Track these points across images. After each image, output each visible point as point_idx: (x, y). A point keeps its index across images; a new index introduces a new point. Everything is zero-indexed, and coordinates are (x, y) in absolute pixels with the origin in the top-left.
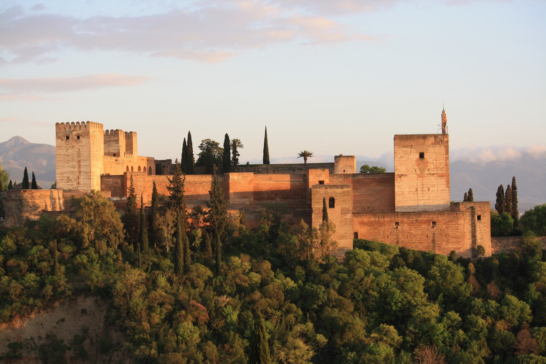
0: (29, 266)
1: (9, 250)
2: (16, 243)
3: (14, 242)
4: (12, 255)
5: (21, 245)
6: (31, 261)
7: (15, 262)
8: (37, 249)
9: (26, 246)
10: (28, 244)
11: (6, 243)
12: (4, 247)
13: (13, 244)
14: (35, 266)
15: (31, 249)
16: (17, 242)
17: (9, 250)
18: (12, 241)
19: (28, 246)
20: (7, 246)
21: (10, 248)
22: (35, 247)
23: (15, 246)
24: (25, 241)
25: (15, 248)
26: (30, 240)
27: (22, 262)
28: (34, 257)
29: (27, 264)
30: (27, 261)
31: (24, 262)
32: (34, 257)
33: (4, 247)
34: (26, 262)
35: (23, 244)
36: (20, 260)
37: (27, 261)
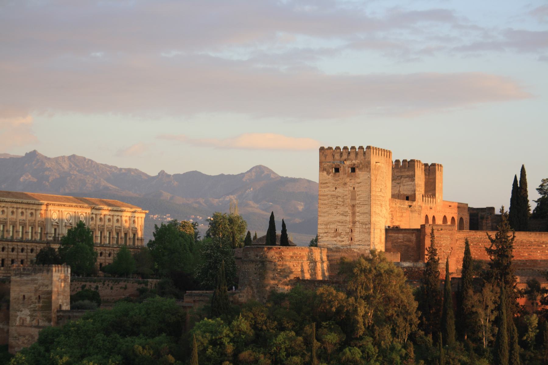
0: (272, 361)
1: (243, 337)
2: (254, 327)
3: (251, 325)
4: (246, 345)
5: (261, 330)
6: (275, 353)
7: (251, 355)
8: (285, 336)
9: (268, 331)
10: (273, 329)
11: (238, 326)
12: (235, 332)
13: (249, 328)
14: (281, 361)
15: (276, 336)
16: (255, 325)
17: (243, 337)
18: (248, 323)
19: (271, 331)
20: (240, 331)
21: (245, 333)
22: (282, 333)
23: (253, 331)
24: (268, 324)
25: (251, 333)
26: (276, 323)
27: (262, 356)
28: (281, 348)
29: (269, 359)
30: (270, 353)
31: (265, 354)
32: (281, 348)
33: (235, 332)
34: (268, 355)
35: (264, 327)
36: (259, 352)
37: (270, 353)
